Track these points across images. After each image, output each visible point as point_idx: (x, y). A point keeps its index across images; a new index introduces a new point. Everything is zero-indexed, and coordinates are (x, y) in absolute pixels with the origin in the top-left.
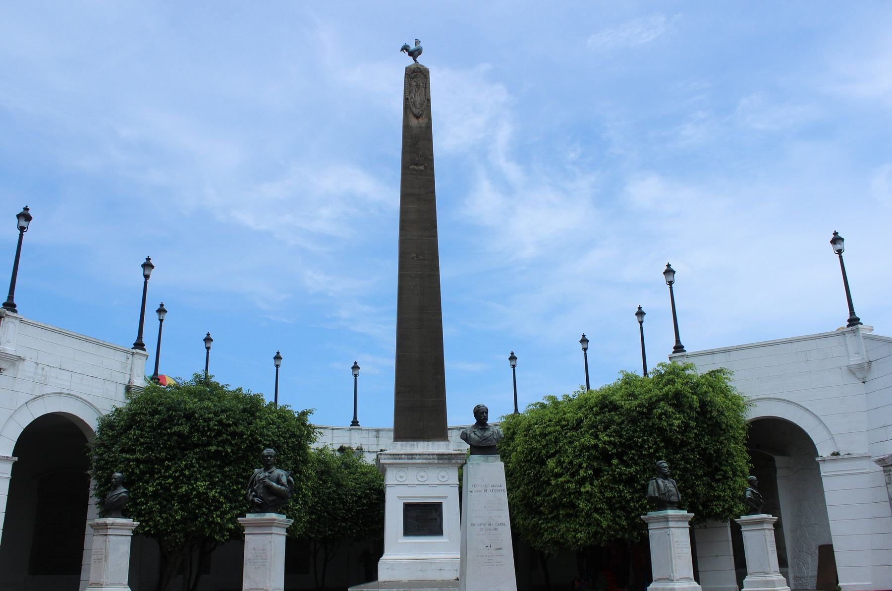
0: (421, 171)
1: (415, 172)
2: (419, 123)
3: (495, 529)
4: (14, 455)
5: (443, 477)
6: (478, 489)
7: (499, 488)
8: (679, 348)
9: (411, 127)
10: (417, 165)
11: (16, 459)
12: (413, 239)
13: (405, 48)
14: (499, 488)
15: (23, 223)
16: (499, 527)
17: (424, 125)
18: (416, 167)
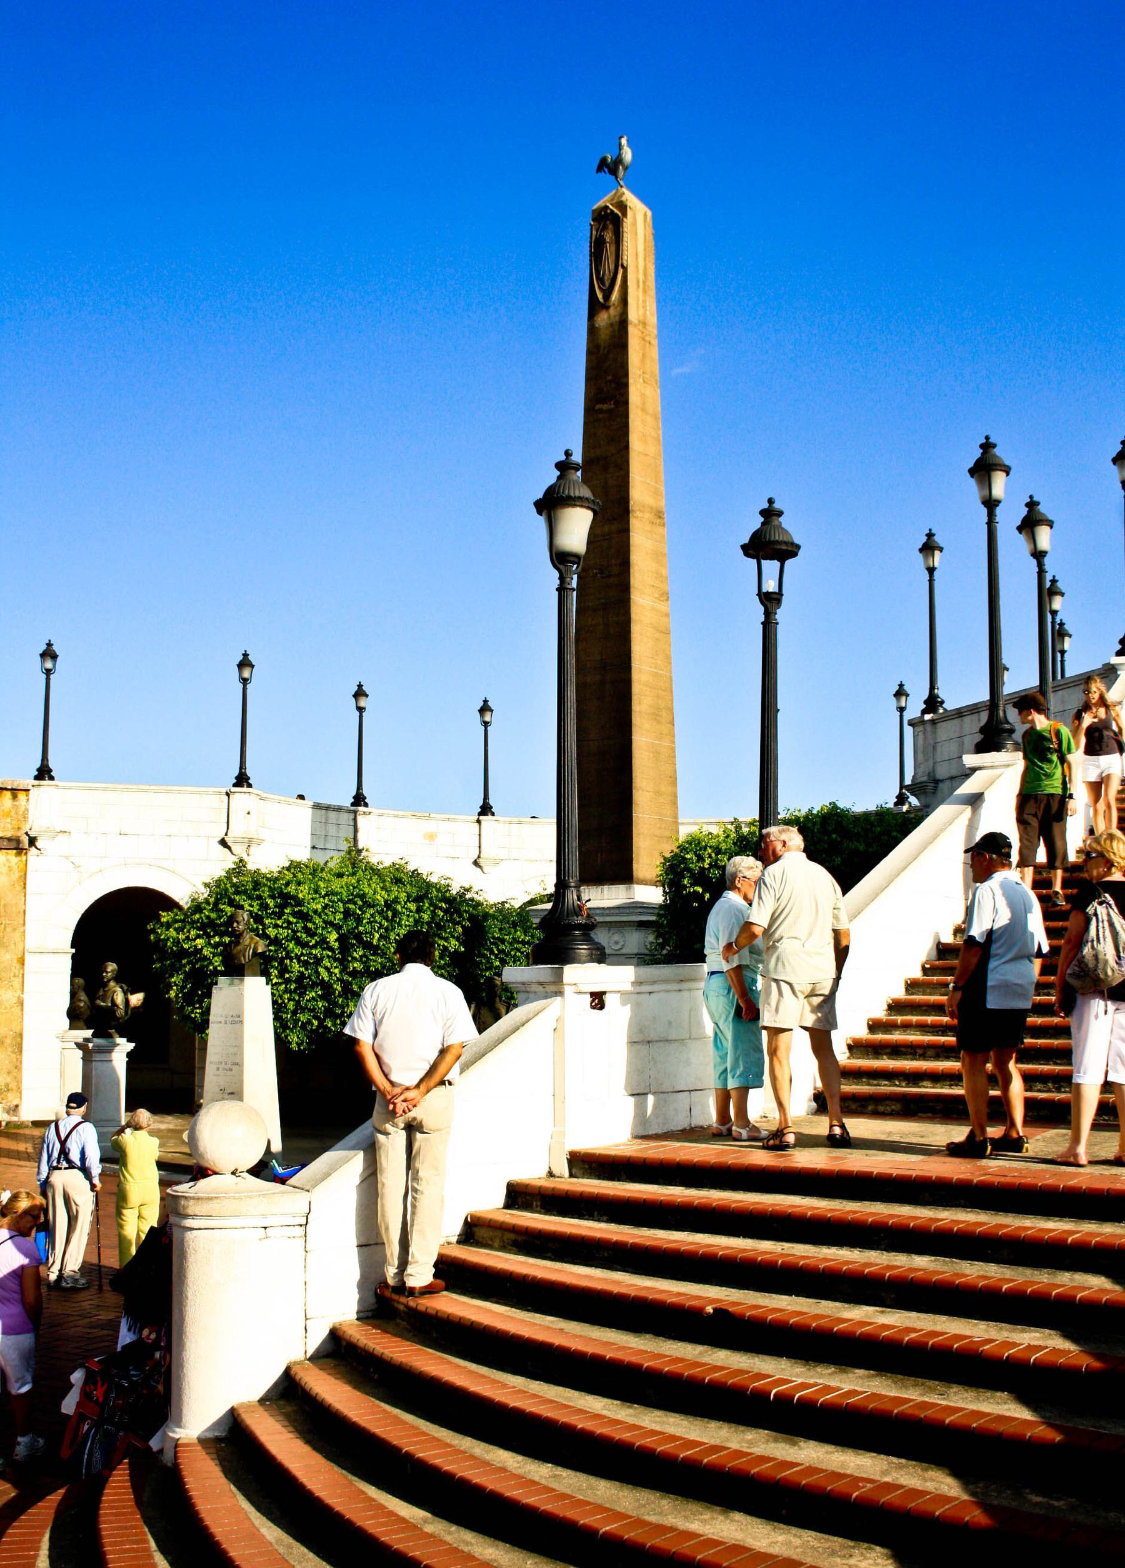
0: (610, 411)
1: (601, 416)
2: (609, 317)
3: (231, 1070)
4: (72, 947)
5: (616, 943)
6: (219, 1019)
7: (238, 1019)
8: (932, 703)
9: (598, 329)
10: (603, 401)
11: (73, 951)
12: (596, 542)
13: (603, 165)
14: (238, 1019)
15: (49, 665)
16: (234, 1067)
17: (617, 319)
18: (605, 407)
